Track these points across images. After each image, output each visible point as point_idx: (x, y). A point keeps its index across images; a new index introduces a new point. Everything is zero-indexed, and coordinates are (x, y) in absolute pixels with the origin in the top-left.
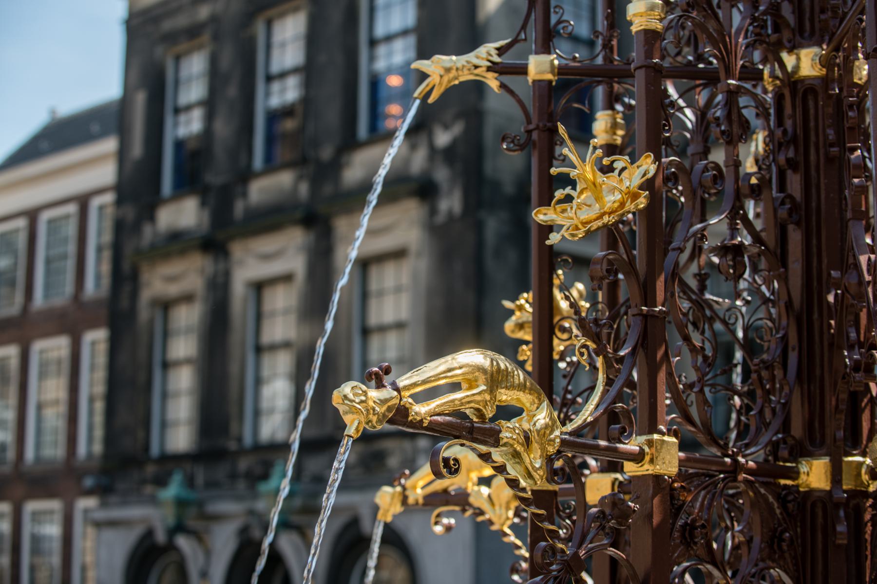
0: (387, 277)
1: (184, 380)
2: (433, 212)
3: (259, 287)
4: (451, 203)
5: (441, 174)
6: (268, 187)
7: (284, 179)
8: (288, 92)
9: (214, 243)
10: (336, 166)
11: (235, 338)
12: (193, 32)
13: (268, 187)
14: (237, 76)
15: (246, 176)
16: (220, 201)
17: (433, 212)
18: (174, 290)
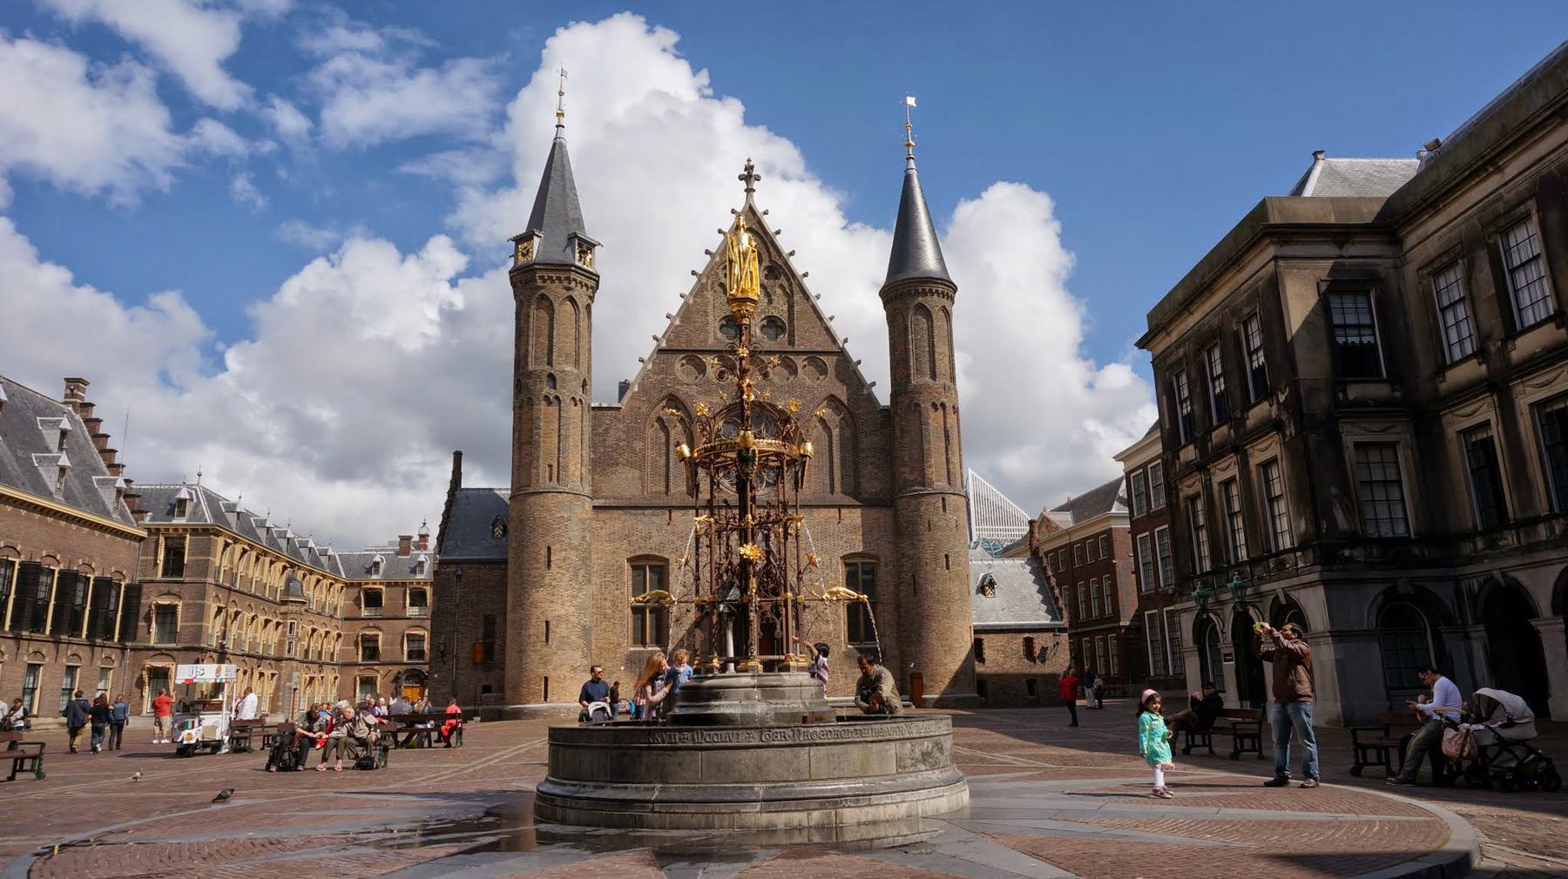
0: (1275, 472)
1: (1203, 536)
2: (1284, 436)
3: (1227, 484)
4: (1291, 430)
5: (1284, 417)
6: (1220, 433)
7: (1224, 429)
8: (1220, 386)
9: (1201, 467)
10: (1244, 420)
11: (1218, 511)
12: (1179, 362)
13: (1220, 433)
14: (1201, 381)
15: (1212, 429)
16: (1202, 444)
17: (1284, 436)
18: (1191, 491)
